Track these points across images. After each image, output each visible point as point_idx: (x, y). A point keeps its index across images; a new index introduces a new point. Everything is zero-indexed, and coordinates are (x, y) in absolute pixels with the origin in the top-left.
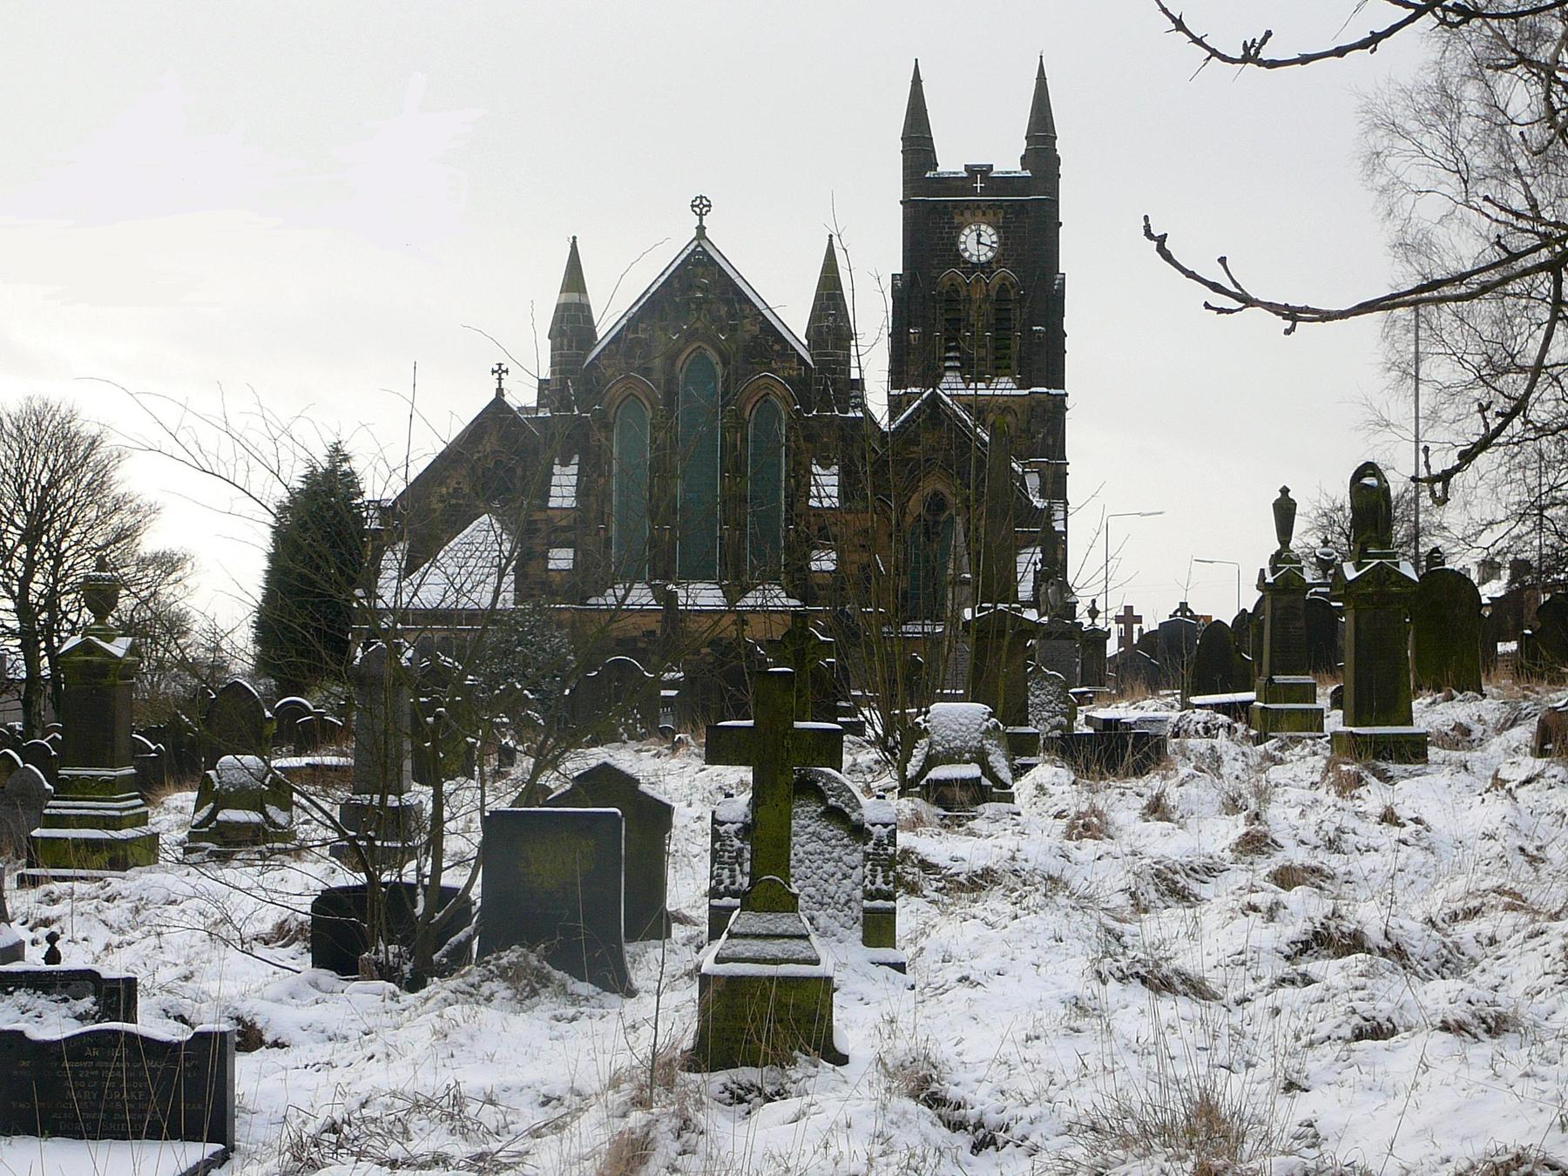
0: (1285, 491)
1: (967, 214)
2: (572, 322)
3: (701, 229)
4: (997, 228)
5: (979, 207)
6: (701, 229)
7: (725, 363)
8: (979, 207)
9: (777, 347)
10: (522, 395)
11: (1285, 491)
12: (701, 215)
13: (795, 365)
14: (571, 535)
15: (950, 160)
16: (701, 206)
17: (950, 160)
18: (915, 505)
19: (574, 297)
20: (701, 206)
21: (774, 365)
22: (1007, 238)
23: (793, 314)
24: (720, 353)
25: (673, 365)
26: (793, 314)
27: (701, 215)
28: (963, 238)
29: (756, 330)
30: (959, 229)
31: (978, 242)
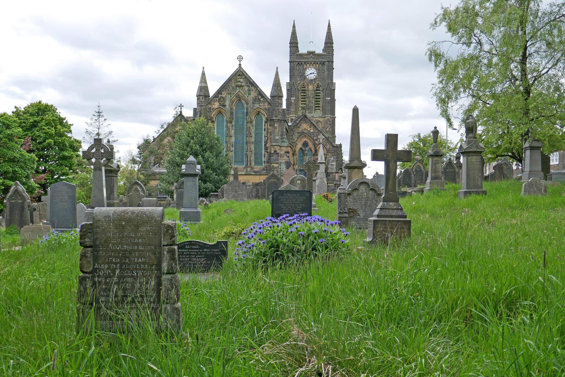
0: (436, 128)
1: (308, 65)
2: (203, 90)
3: (240, 65)
4: (316, 69)
6: (240, 65)
9: (262, 99)
10: (188, 113)
11: (436, 128)
15: (303, 49)
16: (240, 58)
17: (303, 49)
18: (299, 145)
19: (203, 85)
20: (240, 58)
23: (267, 91)
24: (246, 101)
26: (267, 91)
30: (306, 69)
31: (311, 73)
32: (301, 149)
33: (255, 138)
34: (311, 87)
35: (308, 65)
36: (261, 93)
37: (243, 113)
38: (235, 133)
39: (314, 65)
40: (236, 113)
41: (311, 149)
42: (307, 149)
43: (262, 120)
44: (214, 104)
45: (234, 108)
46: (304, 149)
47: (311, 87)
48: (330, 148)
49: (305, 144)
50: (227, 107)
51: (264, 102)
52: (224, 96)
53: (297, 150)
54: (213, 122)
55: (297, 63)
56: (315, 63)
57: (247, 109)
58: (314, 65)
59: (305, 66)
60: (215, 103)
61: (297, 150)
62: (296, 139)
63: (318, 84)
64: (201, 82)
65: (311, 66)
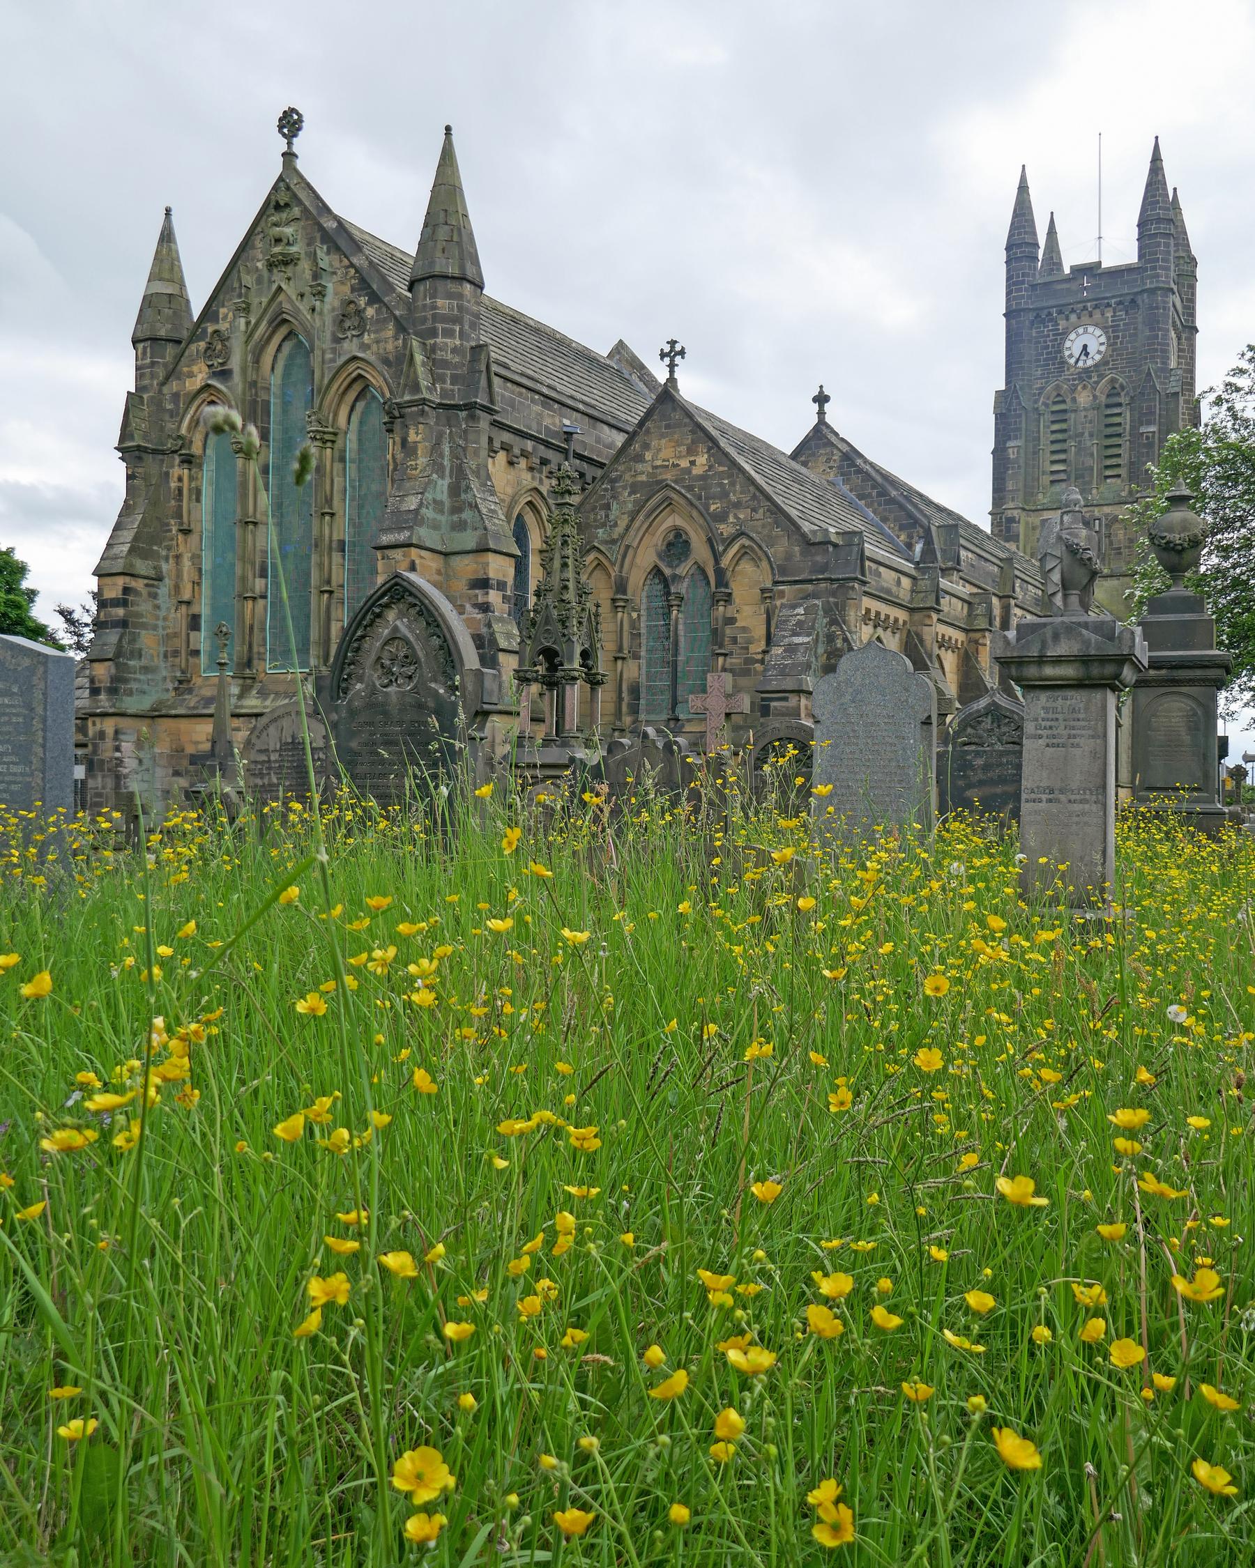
1: (1073, 317)
3: (289, 156)
4: (1105, 329)
6: (289, 156)
9: (370, 312)
14: (120, 612)
16: (290, 123)
18: (646, 556)
20: (290, 123)
25: (257, 361)
28: (1068, 344)
30: (1065, 334)
32: (657, 571)
33: (356, 525)
34: (1084, 398)
35: (1073, 317)
38: (278, 506)
40: (286, 405)
41: (703, 571)
42: (682, 570)
44: (191, 375)
45: (275, 380)
46: (667, 571)
47: (1084, 398)
48: (789, 556)
49: (677, 546)
51: (380, 323)
52: (223, 326)
53: (637, 579)
54: (188, 460)
55: (1031, 316)
56: (1101, 304)
59: (1062, 324)
60: (195, 369)
61: (637, 579)
62: (623, 524)
63: (1113, 380)
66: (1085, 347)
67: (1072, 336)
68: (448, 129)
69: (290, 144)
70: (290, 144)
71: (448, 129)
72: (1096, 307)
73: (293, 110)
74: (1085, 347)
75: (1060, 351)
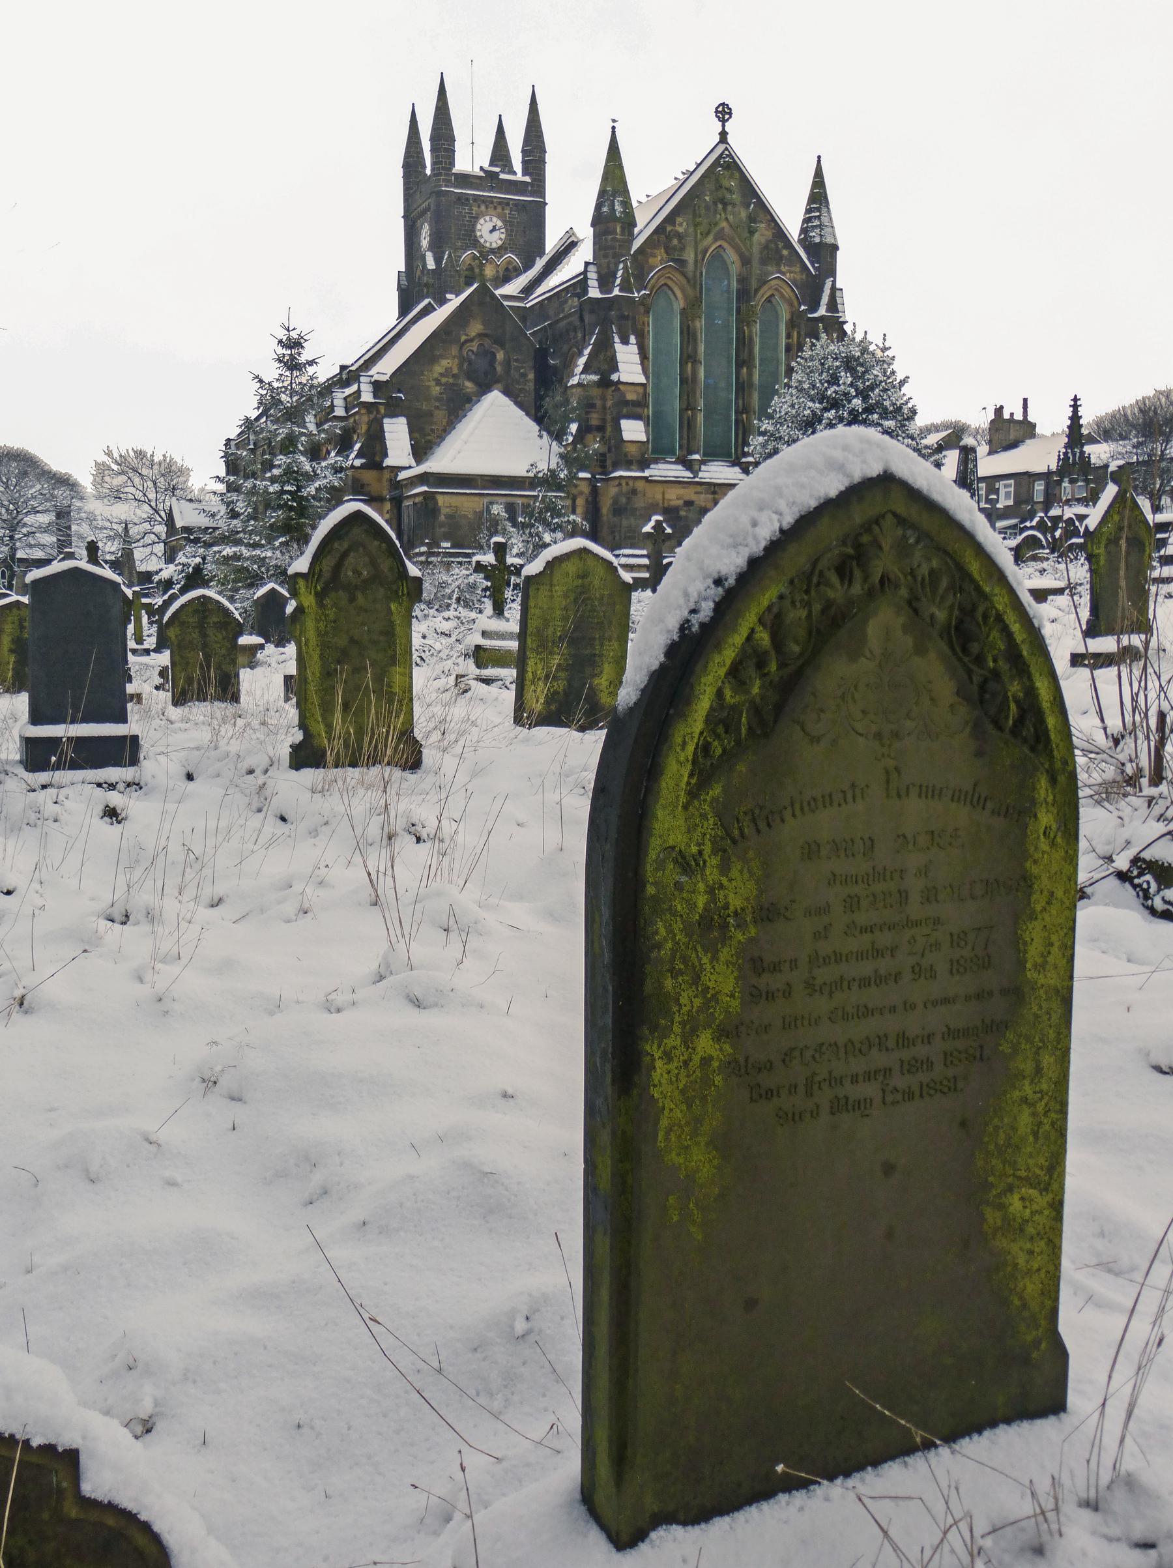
1: (483, 208)
3: (723, 135)
5: (492, 202)
6: (723, 135)
7: (745, 261)
8: (492, 202)
9: (785, 252)
12: (724, 121)
13: (798, 269)
16: (724, 112)
20: (724, 112)
21: (783, 269)
22: (512, 231)
27: (724, 121)
29: (769, 234)
30: (477, 218)
36: (780, 233)
37: (728, 291)
39: (499, 210)
40: (708, 290)
43: (777, 317)
44: (654, 256)
50: (691, 266)
52: (681, 230)
57: (742, 280)
58: (499, 210)
60: (657, 252)
64: (606, 178)
65: (491, 211)
66: (491, 232)
67: (482, 221)
68: (819, 157)
69: (723, 126)
70: (723, 126)
71: (819, 157)
72: (500, 203)
73: (723, 104)
74: (491, 232)
75: (474, 231)
